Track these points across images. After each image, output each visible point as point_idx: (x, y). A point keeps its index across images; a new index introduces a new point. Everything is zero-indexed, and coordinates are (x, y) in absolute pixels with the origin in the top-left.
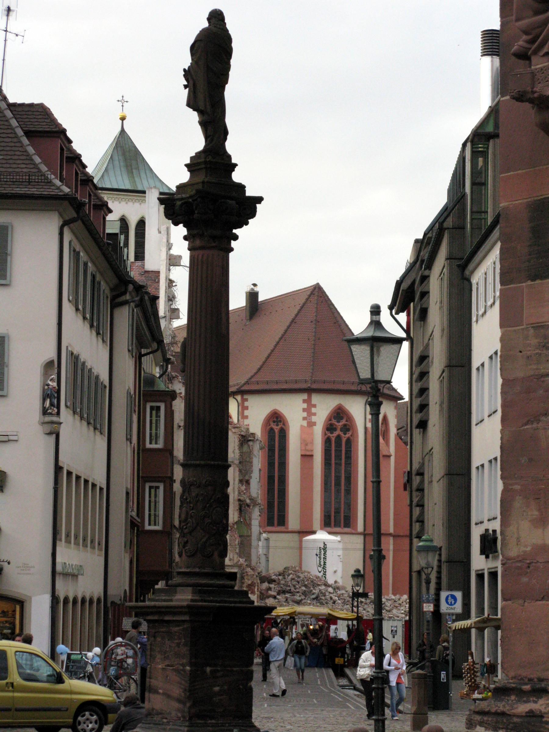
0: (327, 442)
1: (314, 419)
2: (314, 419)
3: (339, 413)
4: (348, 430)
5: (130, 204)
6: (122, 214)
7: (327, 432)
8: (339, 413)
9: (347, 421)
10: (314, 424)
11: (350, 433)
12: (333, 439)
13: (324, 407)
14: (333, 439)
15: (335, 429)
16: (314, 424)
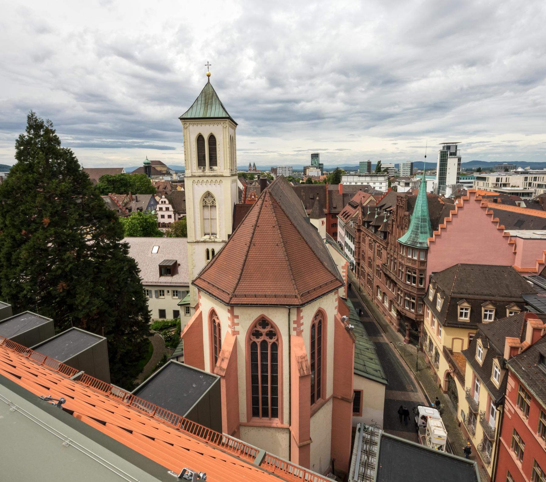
0: (253, 347)
1: (237, 328)
2: (237, 328)
3: (263, 322)
4: (275, 335)
5: (203, 126)
6: (198, 133)
7: (252, 337)
8: (263, 322)
9: (272, 327)
10: (238, 333)
11: (276, 337)
12: (259, 344)
13: (248, 318)
14: (259, 344)
15: (261, 335)
16: (238, 333)
